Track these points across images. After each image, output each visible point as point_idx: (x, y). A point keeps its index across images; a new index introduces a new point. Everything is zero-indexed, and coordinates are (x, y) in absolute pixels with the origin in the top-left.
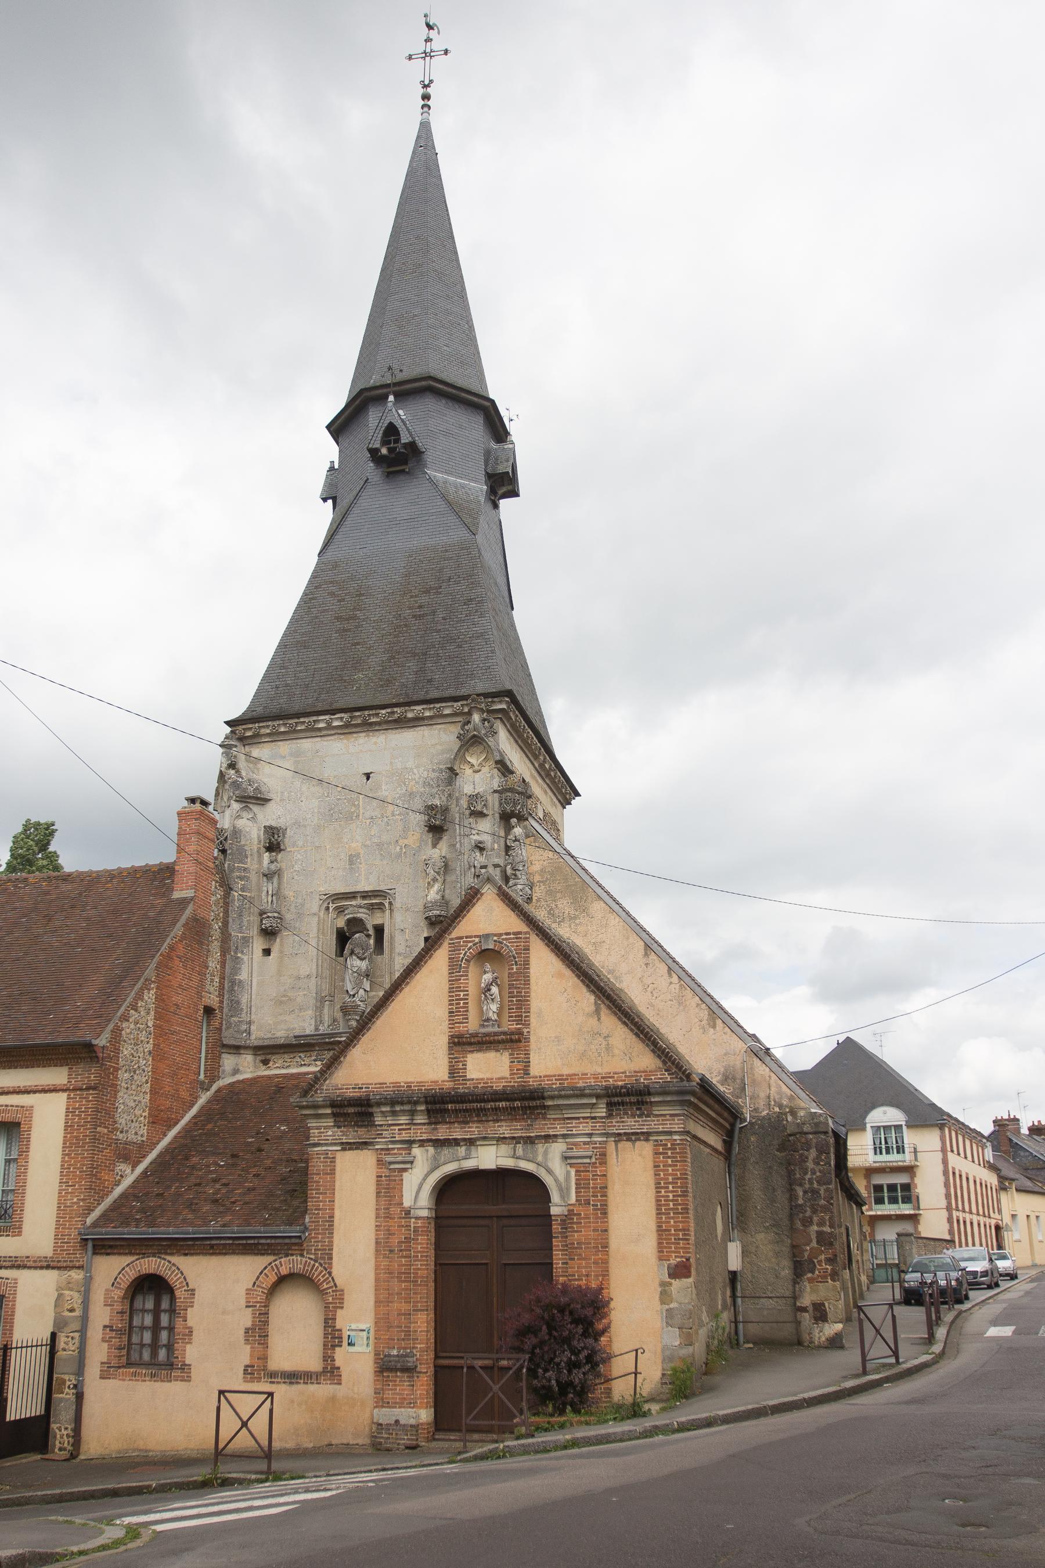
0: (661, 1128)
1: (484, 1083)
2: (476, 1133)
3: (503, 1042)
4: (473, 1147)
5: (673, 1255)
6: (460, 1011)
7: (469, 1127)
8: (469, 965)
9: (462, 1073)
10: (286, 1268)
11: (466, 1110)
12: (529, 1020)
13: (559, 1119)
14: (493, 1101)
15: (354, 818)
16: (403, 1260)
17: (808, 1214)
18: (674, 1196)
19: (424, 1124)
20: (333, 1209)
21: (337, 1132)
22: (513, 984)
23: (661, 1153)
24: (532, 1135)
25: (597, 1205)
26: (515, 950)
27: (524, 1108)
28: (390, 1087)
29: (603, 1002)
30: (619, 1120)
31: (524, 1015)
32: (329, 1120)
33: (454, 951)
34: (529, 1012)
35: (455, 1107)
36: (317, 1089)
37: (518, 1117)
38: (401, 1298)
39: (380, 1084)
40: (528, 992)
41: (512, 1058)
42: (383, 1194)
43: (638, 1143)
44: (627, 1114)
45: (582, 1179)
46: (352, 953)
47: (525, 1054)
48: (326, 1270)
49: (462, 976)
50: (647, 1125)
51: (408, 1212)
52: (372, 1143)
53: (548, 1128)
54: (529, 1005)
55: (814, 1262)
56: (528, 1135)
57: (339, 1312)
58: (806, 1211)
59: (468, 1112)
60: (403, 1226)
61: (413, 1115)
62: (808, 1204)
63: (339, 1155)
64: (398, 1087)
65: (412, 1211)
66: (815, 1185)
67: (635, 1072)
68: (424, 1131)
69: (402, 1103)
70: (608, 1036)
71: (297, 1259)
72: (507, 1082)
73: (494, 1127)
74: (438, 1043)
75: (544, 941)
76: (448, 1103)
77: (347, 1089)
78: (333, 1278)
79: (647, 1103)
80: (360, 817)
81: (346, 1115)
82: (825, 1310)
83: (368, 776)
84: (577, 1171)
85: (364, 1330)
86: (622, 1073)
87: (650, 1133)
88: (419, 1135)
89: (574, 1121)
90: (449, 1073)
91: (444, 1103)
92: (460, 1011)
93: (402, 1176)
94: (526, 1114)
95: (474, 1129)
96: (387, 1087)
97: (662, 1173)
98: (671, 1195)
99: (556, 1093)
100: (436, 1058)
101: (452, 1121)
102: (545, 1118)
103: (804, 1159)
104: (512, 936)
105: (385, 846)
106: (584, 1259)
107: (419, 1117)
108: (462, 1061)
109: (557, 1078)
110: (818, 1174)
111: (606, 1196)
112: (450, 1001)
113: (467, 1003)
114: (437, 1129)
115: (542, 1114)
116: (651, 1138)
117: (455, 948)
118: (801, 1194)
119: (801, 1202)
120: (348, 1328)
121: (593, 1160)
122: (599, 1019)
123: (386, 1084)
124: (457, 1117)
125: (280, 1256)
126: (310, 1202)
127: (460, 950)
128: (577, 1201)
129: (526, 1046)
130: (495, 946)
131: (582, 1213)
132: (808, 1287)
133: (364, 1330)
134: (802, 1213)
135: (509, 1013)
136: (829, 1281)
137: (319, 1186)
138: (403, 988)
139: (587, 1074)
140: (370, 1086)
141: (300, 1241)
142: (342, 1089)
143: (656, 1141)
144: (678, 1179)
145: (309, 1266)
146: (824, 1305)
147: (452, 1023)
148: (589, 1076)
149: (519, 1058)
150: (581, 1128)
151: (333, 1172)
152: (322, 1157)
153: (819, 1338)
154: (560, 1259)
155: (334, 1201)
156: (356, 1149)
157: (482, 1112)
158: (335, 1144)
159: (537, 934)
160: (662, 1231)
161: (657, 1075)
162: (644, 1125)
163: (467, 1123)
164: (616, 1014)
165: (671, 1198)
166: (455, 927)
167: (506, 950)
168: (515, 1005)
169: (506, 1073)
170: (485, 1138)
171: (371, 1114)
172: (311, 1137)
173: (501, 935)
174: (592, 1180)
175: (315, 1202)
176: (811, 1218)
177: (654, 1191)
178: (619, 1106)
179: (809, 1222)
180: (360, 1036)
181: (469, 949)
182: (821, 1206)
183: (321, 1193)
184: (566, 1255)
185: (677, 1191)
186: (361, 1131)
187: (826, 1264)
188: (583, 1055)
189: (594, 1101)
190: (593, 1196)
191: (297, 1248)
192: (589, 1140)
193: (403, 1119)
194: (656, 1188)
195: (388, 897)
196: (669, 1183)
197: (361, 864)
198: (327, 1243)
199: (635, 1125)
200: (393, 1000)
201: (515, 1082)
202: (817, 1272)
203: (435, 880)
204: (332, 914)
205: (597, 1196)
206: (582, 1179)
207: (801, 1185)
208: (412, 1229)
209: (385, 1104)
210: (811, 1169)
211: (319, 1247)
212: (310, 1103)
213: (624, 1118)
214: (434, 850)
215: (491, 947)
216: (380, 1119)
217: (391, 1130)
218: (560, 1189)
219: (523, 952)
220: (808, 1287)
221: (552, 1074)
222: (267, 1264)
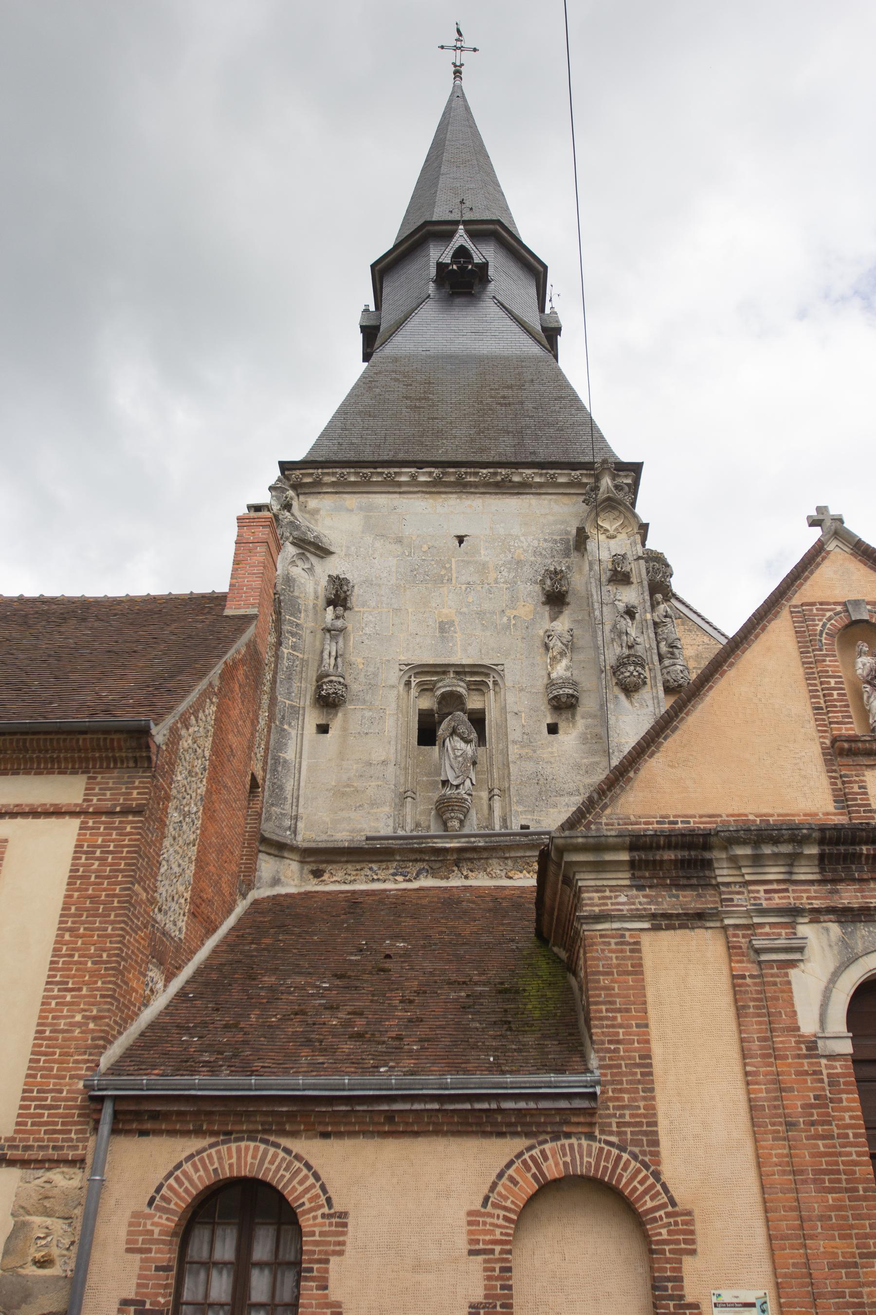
9: (861, 799)
10: (557, 1164)
15: (445, 581)
16: (820, 1143)
19: (812, 882)
20: (648, 1042)
21: (637, 897)
32: (620, 875)
36: (590, 823)
42: (751, 1010)
46: (454, 732)
48: (647, 1167)
49: (827, 655)
51: (812, 1046)
52: (716, 915)
57: (688, 1262)
60: (806, 1073)
61: (791, 865)
63: (646, 940)
65: (820, 1043)
69: (776, 841)
71: (580, 1145)
74: (803, 754)
76: (861, 842)
77: (646, 823)
78: (664, 1186)
80: (454, 581)
81: (656, 865)
83: (461, 539)
92: (835, 706)
93: (786, 975)
100: (805, 777)
101: (865, 877)
105: (488, 615)
107: (803, 870)
108: (856, 782)
114: (837, 891)
123: (720, 816)
125: (541, 1138)
126: (596, 1027)
127: (814, 620)
137: (611, 995)
138: (725, 671)
140: (691, 820)
141: (593, 1105)
142: (637, 823)
145: (607, 1160)
147: (823, 726)
151: (638, 970)
152: (613, 941)
155: (647, 1026)
156: (682, 927)
158: (640, 918)
171: (708, 864)
172: (587, 905)
175: (608, 1026)
180: (661, 740)
183: (619, 1011)
186: (684, 897)
191: (582, 1119)
193: (774, 873)
195: (492, 674)
197: (455, 632)
198: (642, 1111)
200: (711, 688)
203: (562, 654)
204: (414, 692)
208: (826, 1080)
209: (744, 843)
211: (627, 1119)
212: (591, 840)
214: (555, 623)
215: (866, 617)
216: (725, 872)
217: (749, 892)
222: (512, 1157)
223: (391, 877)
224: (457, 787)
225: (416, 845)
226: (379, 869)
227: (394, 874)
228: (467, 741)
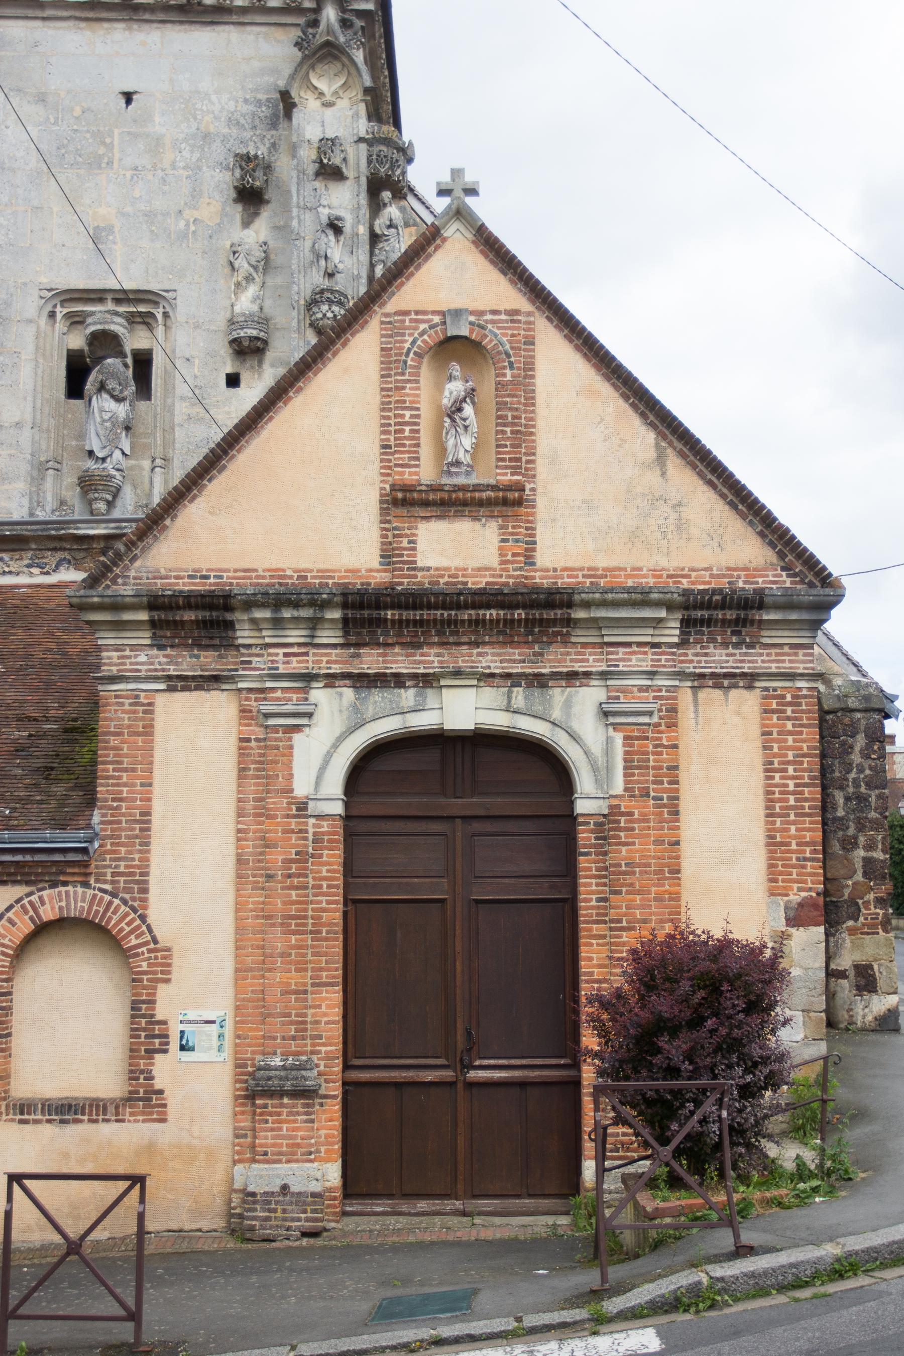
0: (773, 668)
1: (449, 576)
2: (436, 664)
3: (489, 503)
4: (429, 692)
5: (795, 886)
6: (404, 445)
7: (422, 655)
8: (420, 363)
9: (408, 556)
10: (53, 908)
11: (420, 623)
12: (534, 469)
13: (593, 645)
14: (474, 606)
15: (103, 165)
16: (293, 893)
17: (851, 831)
18: (796, 785)
19: (334, 646)
20: (149, 800)
21: (157, 657)
22: (506, 403)
23: (773, 711)
24: (544, 671)
25: (661, 799)
26: (510, 342)
27: (530, 623)
28: (264, 577)
29: (671, 444)
30: (699, 650)
31: (524, 459)
32: (140, 634)
33: (391, 336)
34: (534, 454)
35: (400, 615)
36: (117, 576)
37: (516, 639)
38: (290, 963)
39: (245, 571)
40: (532, 419)
41: (504, 534)
42: (251, 772)
43: (733, 693)
44: (714, 641)
45: (636, 753)
46: (101, 387)
47: (527, 529)
48: (134, 910)
49: (408, 381)
50: (750, 662)
51: (302, 807)
52: (231, 679)
53: (572, 661)
54: (534, 441)
55: (857, 904)
56: (536, 671)
57: (162, 989)
58: (847, 828)
59: (421, 626)
60: (293, 832)
61: (314, 628)
62: (852, 817)
63: (161, 700)
64: (280, 577)
65: (311, 804)
66: (863, 789)
67: (729, 569)
68: (334, 658)
69: (296, 605)
70: (680, 504)
71: (75, 893)
72: (493, 576)
73: (471, 655)
74: (359, 501)
75: (561, 330)
76: (386, 608)
77: (177, 577)
78: (149, 928)
79: (752, 622)
80: (116, 165)
81: (178, 625)
82: (873, 976)
83: (128, 97)
84: (626, 738)
85: (213, 1022)
86: (705, 569)
87: (758, 675)
88: (324, 665)
89: (621, 650)
90: (382, 557)
91: (378, 607)
92: (404, 445)
93: (290, 739)
94: (531, 633)
95: (431, 658)
96: (258, 577)
97: (775, 746)
98: (791, 783)
99: (597, 596)
100: (355, 528)
101: (390, 641)
102: (566, 643)
103: (847, 749)
104: (503, 317)
105: (160, 218)
106: (639, 892)
107: (327, 633)
108: (406, 535)
109: (585, 572)
110: (868, 772)
111: (677, 783)
112: (383, 425)
113: (418, 431)
114: (358, 655)
115: (562, 635)
116: (758, 684)
117: (393, 330)
118: (841, 801)
119: (840, 813)
120: (181, 1018)
121: (655, 719)
122: (663, 474)
123: (256, 570)
124: (400, 634)
125: (40, 886)
126: (102, 785)
127: (403, 335)
128: (626, 789)
129: (528, 514)
130: (472, 332)
131: (636, 812)
132: (848, 941)
133: (213, 1022)
134: (843, 830)
135: (498, 453)
136: (880, 931)
137: (119, 755)
138: (290, 399)
139: (640, 569)
140: (225, 575)
141: (86, 858)
142: (167, 577)
143: (766, 689)
144: (804, 756)
145: (99, 905)
146: (871, 967)
147: (387, 467)
148: (645, 572)
149: (517, 534)
150: (634, 662)
151: (148, 731)
152: (127, 701)
153: (864, 1017)
154: (593, 892)
155: (150, 785)
156: (197, 688)
157: (449, 626)
158: (156, 679)
159: (548, 318)
160: (774, 844)
161: (767, 576)
162: (743, 661)
163: (419, 646)
164: (694, 467)
165: (791, 788)
166: (393, 294)
167: (491, 341)
168: (508, 438)
169: (494, 561)
170: (457, 673)
171: (230, 625)
172: (105, 664)
173: (480, 313)
174: (654, 753)
175: (113, 785)
176: (856, 838)
177: (762, 775)
178: (702, 626)
179: (851, 844)
180: (205, 482)
181: (422, 334)
182: (871, 821)
183: (126, 770)
184: (605, 885)
185: (802, 778)
186: (206, 657)
187: (875, 907)
188: (634, 535)
189: (663, 614)
190: (654, 782)
191: (76, 870)
192: (648, 683)
193: (295, 636)
194: (767, 770)
195: (163, 303)
196: (789, 763)
197: (115, 243)
198: (137, 863)
199: (727, 662)
200: (271, 418)
201: (509, 577)
202: (861, 919)
203: (249, 279)
204: (60, 325)
205: (662, 783)
206: (636, 753)
207: (842, 788)
208: (311, 837)
209: (263, 605)
210: (857, 765)
211: (122, 869)
212: (107, 600)
213: (708, 648)
214: (246, 231)
215: (464, 331)
216: (246, 634)
217: (269, 655)
218: (595, 769)
219: (523, 347)
220: (848, 941)
221: (577, 565)
222: (12, 902)
223: (25, 569)
224: (104, 460)
225: (53, 532)
226: (12, 559)
227: (29, 566)
228: (118, 399)
